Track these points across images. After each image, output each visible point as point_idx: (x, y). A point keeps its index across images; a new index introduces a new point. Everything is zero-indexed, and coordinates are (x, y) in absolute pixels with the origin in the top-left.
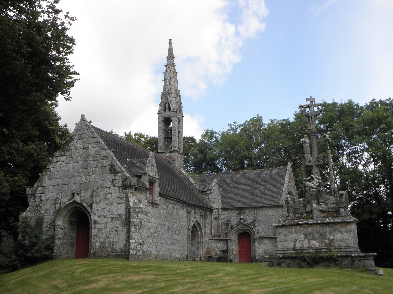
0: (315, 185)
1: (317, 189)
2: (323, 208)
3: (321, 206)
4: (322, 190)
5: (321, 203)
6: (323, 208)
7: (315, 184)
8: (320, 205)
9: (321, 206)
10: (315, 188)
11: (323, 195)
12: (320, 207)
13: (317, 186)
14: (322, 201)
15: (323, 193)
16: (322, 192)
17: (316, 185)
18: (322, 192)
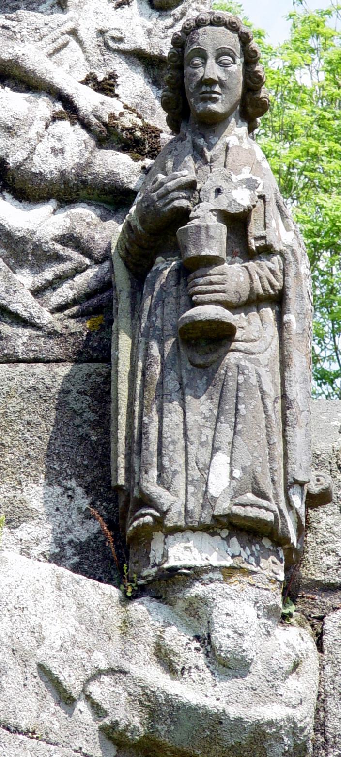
0: (69, 109)
1: (113, 198)
2: (230, 666)
3: (197, 616)
4: (237, 223)
5: (181, 553)
6: (230, 666)
7: (69, 80)
8: (166, 585)
9: (177, 638)
10: (67, 191)
11: (255, 330)
12: (164, 657)
13: (108, 135)
14: (219, 480)
15: (252, 302)
16: (235, 276)
17: (88, 100)
18: (235, 276)
